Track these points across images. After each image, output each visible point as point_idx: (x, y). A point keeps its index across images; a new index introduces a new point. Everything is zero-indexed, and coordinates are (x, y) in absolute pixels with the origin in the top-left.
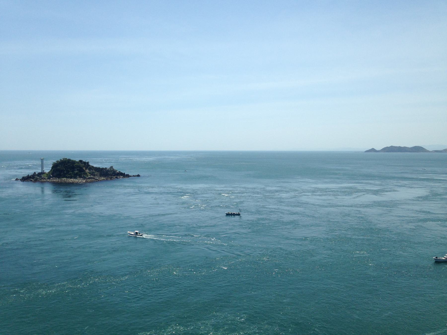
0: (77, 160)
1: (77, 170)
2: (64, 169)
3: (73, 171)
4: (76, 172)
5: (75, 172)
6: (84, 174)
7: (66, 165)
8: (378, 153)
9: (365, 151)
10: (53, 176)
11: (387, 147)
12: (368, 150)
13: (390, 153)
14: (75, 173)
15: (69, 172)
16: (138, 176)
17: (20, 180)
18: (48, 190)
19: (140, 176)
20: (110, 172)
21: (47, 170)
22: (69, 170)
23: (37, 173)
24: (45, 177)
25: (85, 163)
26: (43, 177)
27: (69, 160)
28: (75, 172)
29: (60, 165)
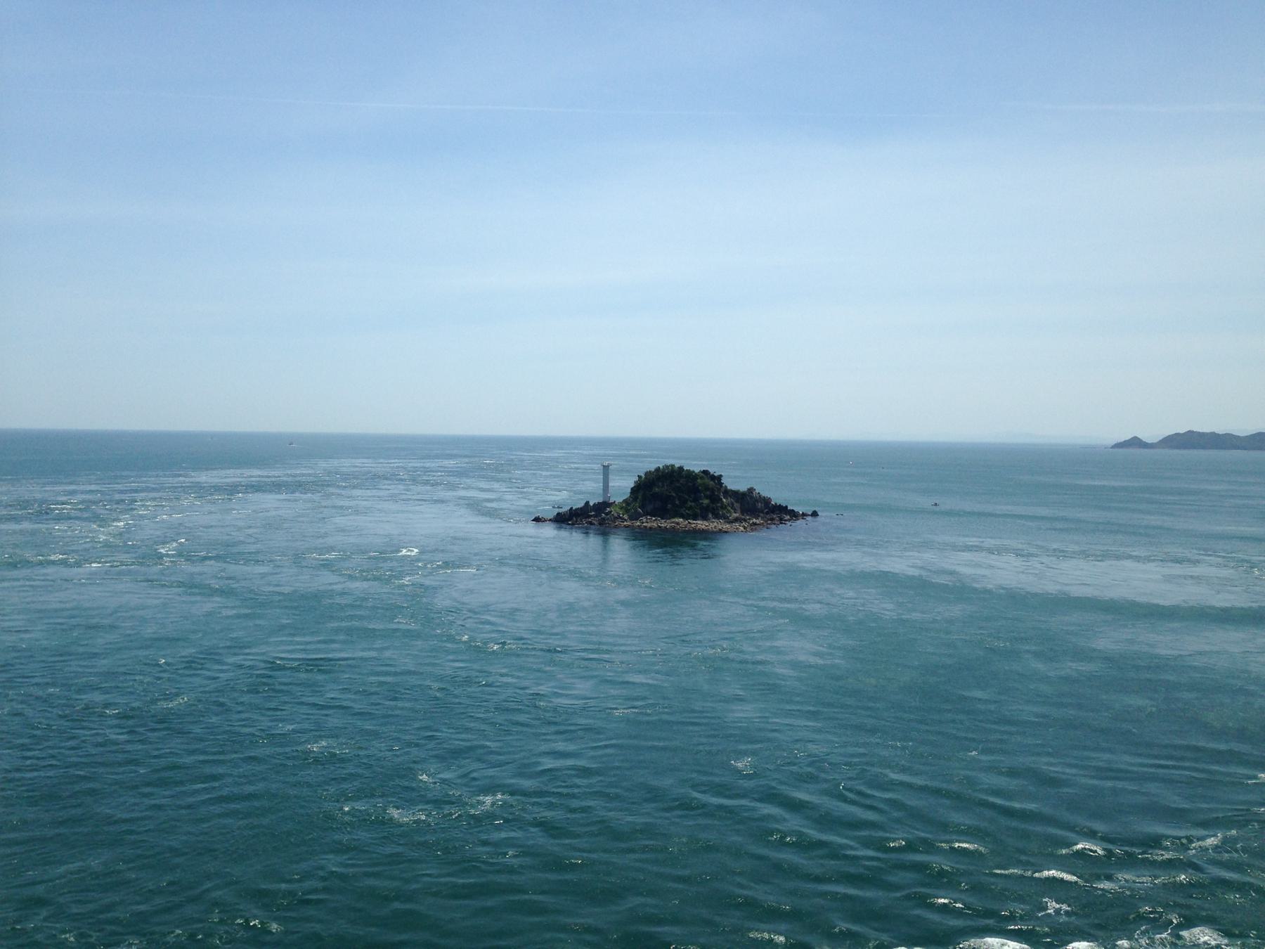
0: (697, 470)
1: (707, 497)
2: (674, 495)
3: (696, 500)
4: (706, 502)
5: (701, 501)
7: (678, 485)
8: (1152, 451)
9: (1114, 443)
10: (646, 514)
12: (1123, 440)
15: (685, 502)
16: (815, 514)
17: (550, 520)
18: (620, 547)
20: (760, 504)
22: (687, 497)
23: (591, 504)
24: (621, 515)
25: (713, 478)
26: (616, 515)
27: (681, 468)
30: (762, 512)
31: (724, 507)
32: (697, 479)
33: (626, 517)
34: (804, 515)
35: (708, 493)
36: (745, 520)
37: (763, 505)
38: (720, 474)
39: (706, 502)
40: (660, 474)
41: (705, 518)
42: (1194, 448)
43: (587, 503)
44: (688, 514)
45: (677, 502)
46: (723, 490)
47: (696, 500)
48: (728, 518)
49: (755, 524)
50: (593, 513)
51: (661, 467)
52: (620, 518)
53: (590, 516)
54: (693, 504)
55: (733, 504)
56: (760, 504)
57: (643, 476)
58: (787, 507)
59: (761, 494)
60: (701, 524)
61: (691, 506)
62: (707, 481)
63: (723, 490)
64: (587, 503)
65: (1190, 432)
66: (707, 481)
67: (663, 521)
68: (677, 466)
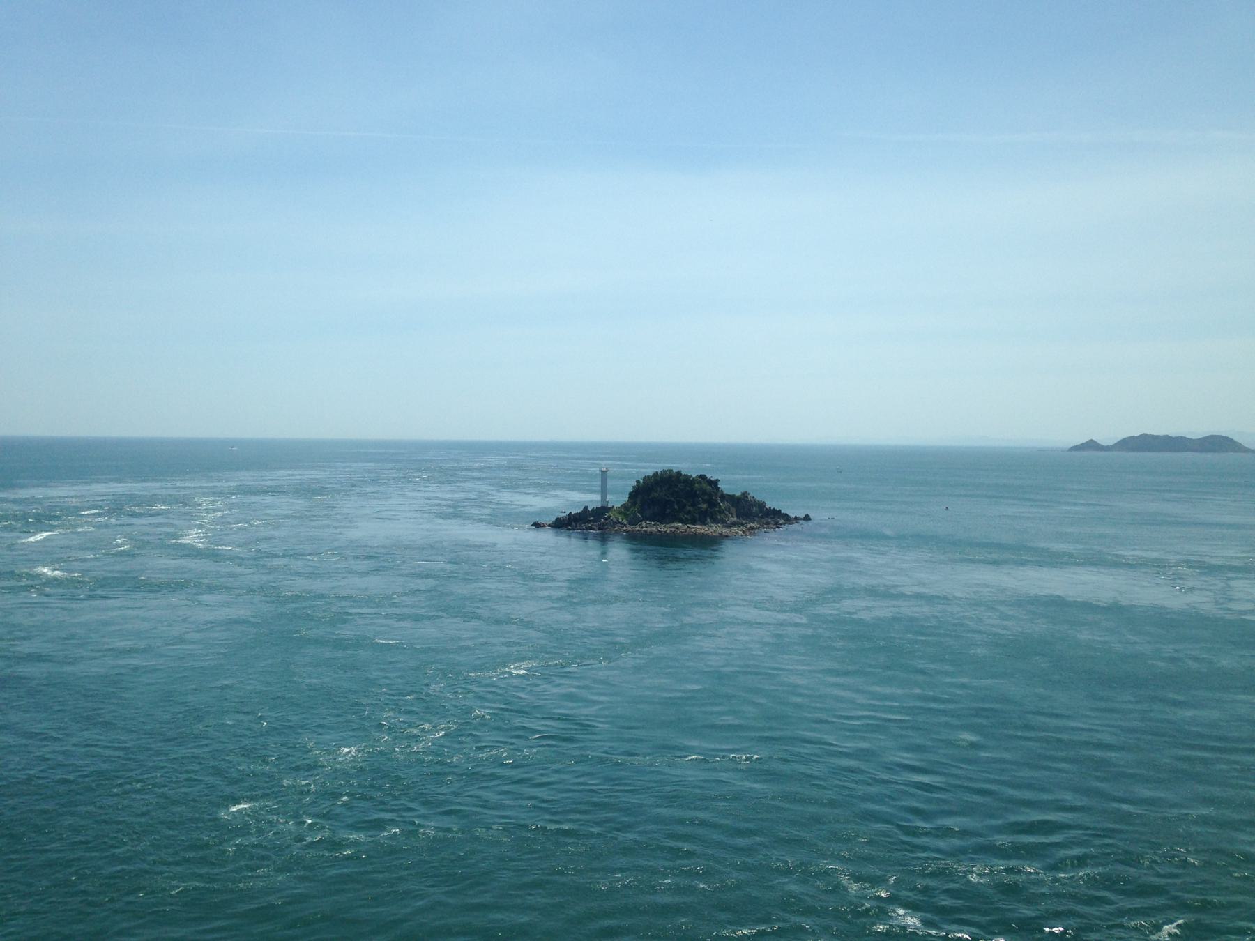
1: (705, 502)
2: (672, 499)
5: (699, 506)
6: (720, 512)
7: (676, 489)
10: (645, 519)
11: (1133, 438)
12: (1079, 443)
13: (1204, 455)
14: (703, 510)
16: (807, 518)
17: (549, 525)
19: (810, 519)
20: (754, 508)
21: (618, 499)
24: (620, 520)
26: (615, 520)
27: (679, 473)
28: (701, 508)
29: (659, 489)
30: (757, 516)
31: (721, 512)
32: (695, 483)
33: (625, 522)
34: (797, 519)
35: (706, 497)
36: (742, 525)
37: (757, 509)
38: (716, 478)
39: (704, 506)
40: (658, 479)
41: (704, 523)
42: (1149, 450)
43: (586, 508)
44: (686, 518)
45: (676, 507)
46: (719, 494)
47: (693, 505)
48: (725, 522)
49: (752, 528)
50: (592, 518)
51: (659, 472)
52: (619, 523)
53: (589, 521)
54: (691, 509)
55: (729, 509)
56: (754, 508)
57: (642, 481)
58: (780, 511)
59: (755, 497)
60: (700, 529)
61: (689, 511)
62: (705, 485)
63: (719, 494)
64: (586, 508)
65: (1145, 435)
66: (705, 485)
67: (662, 526)
68: (675, 471)
